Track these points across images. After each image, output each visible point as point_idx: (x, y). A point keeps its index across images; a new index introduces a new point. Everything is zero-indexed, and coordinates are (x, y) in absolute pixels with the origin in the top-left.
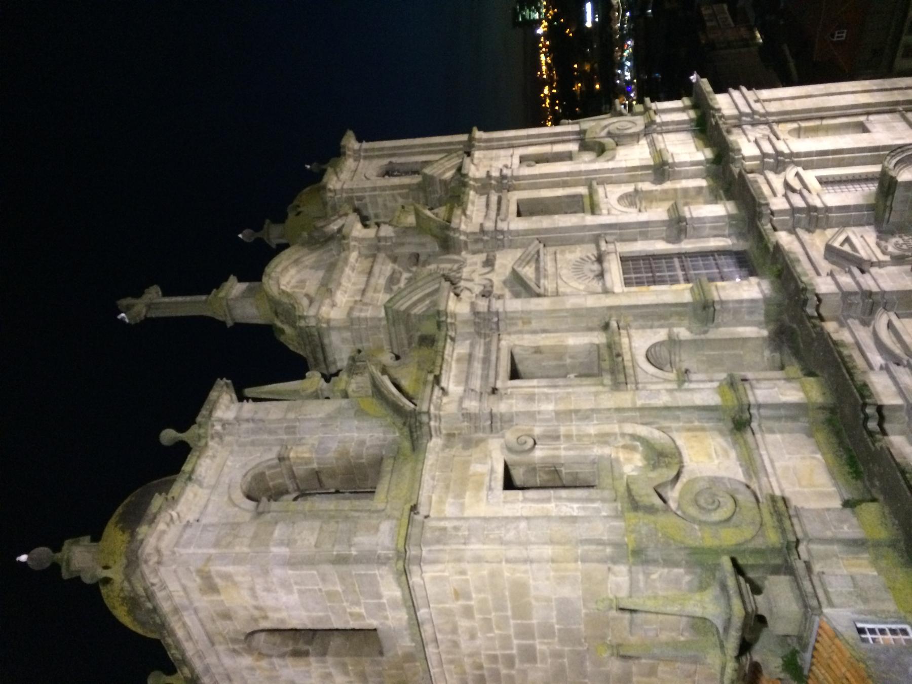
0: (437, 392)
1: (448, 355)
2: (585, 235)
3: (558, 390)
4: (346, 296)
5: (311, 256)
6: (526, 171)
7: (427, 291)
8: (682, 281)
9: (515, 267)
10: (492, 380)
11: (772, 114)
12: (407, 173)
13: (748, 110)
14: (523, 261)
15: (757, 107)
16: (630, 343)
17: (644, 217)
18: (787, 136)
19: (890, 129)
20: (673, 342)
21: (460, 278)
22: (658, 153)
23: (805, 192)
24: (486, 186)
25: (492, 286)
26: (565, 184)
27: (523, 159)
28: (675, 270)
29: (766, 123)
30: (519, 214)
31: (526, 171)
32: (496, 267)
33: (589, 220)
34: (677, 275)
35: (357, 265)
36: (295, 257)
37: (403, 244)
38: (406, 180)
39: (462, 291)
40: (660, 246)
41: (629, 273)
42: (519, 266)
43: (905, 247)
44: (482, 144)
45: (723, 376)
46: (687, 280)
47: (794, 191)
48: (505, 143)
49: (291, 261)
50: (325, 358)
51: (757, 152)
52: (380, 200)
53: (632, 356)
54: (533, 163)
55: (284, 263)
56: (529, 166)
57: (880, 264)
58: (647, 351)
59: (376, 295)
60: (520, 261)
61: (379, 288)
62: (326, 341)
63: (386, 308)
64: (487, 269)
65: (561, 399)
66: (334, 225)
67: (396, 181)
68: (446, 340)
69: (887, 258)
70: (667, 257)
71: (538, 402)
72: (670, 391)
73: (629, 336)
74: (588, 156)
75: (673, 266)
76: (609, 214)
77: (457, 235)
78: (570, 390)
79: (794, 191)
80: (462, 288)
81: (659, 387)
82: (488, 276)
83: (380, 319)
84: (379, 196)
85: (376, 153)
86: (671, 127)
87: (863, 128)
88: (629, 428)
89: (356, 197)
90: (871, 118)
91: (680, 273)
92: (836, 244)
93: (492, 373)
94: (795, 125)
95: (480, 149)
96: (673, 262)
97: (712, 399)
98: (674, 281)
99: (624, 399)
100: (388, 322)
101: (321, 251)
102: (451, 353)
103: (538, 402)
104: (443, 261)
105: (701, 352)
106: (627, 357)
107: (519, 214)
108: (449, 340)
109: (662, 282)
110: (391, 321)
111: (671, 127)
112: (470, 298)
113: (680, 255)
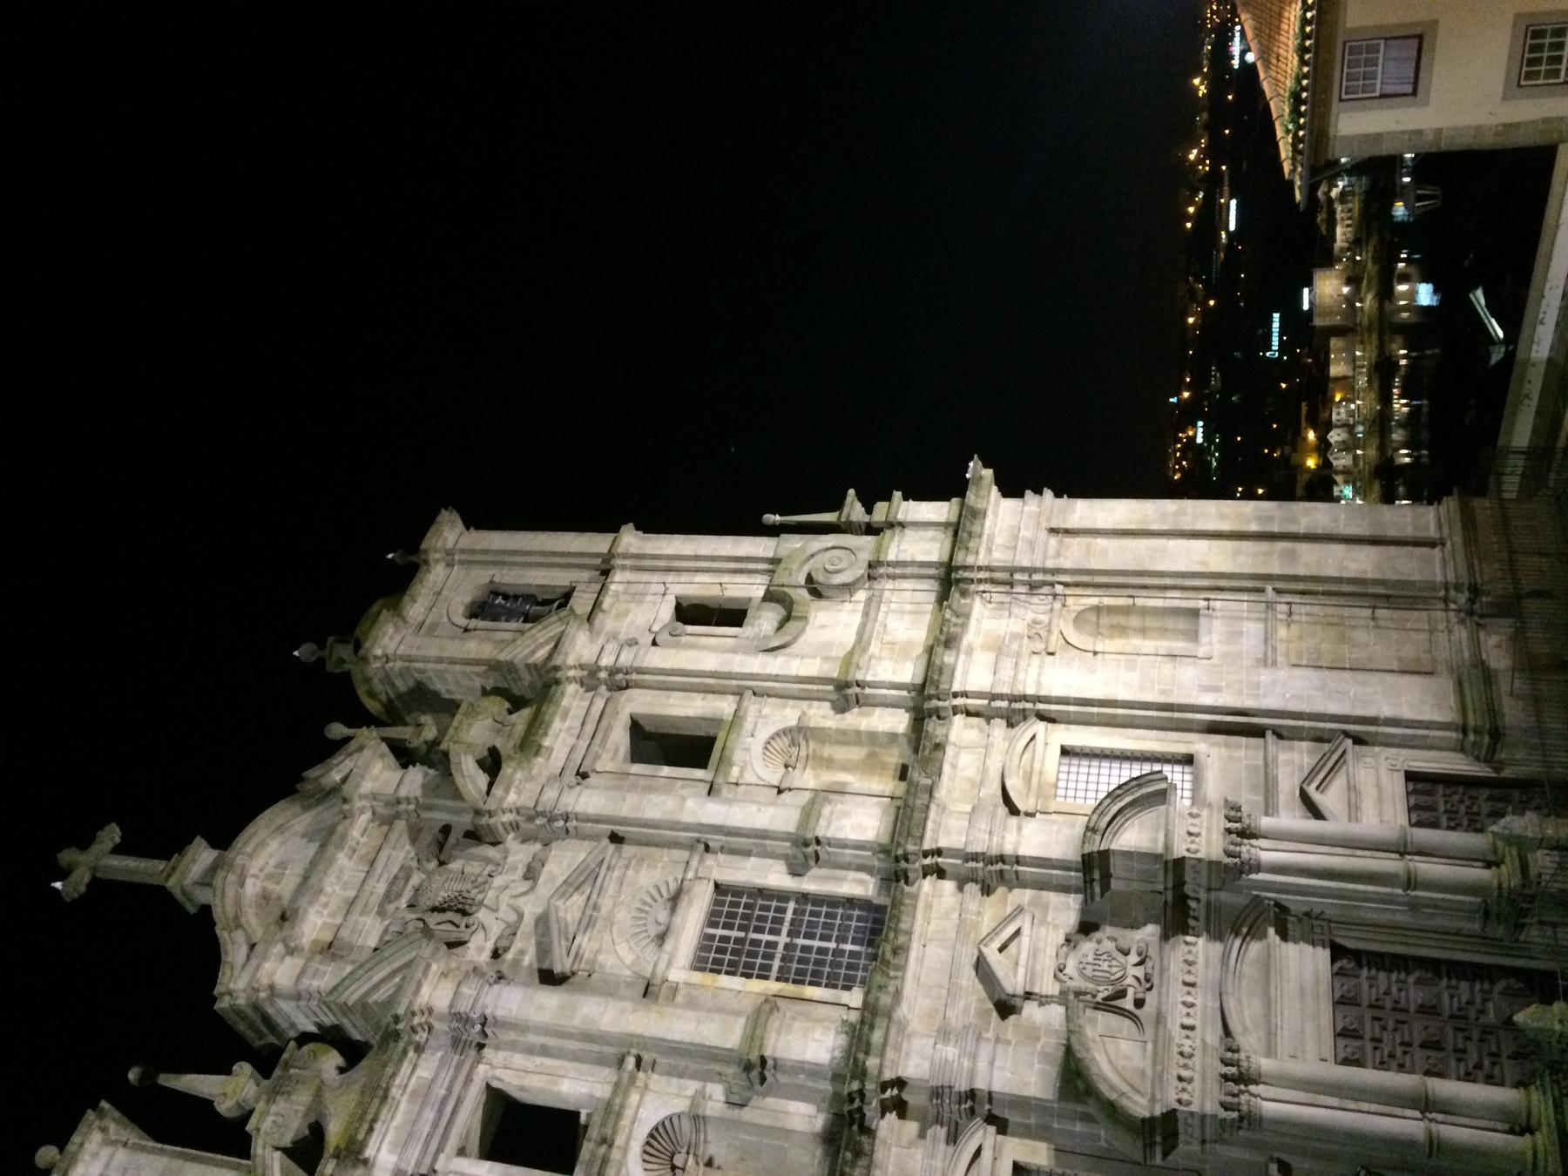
4: (326, 912)
5: (303, 817)
21: (481, 903)
24: (591, 678)
35: (363, 840)
36: (279, 821)
37: (430, 808)
44: (628, 562)
48: (662, 563)
49: (273, 828)
55: (262, 834)
59: (363, 919)
61: (371, 904)
84: (445, 671)
86: (909, 571)
95: (624, 568)
101: (320, 808)
104: (474, 858)
111: (909, 571)
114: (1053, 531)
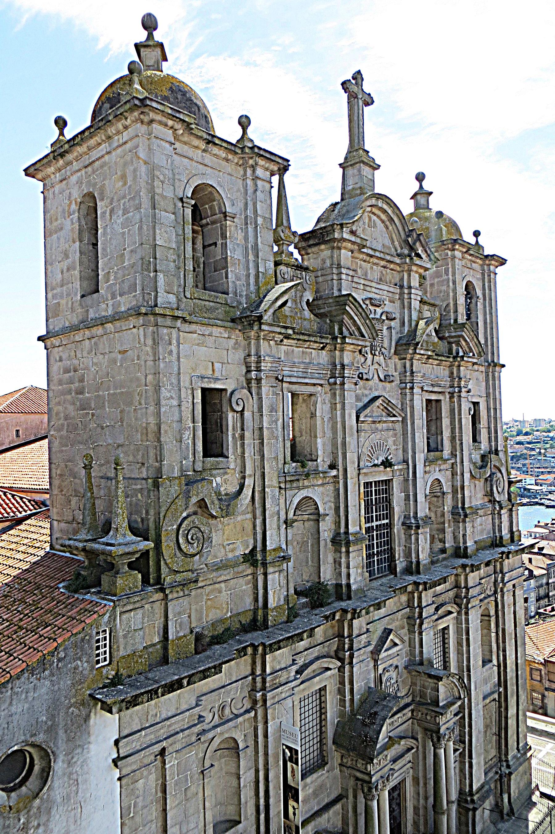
0: (278, 337)
1: (310, 345)
2: (408, 453)
3: (280, 430)
6: (466, 406)
7: (362, 327)
8: (368, 525)
9: (382, 398)
10: (288, 380)
11: (502, 597)
12: (468, 309)
13: (506, 579)
14: (387, 404)
15: (510, 585)
16: (318, 485)
17: (421, 498)
18: (483, 608)
19: (486, 681)
20: (317, 517)
22: (475, 511)
23: (436, 617)
25: (367, 380)
26: (453, 439)
27: (476, 404)
28: (377, 520)
29: (495, 592)
30: (429, 401)
31: (466, 406)
32: (384, 383)
33: (420, 457)
34: (372, 521)
38: (462, 310)
39: (364, 355)
40: (398, 510)
41: (375, 486)
42: (383, 400)
43: (388, 684)
45: (290, 552)
46: (368, 530)
47: (437, 609)
51: (470, 584)
52: (444, 288)
53: (307, 487)
54: (472, 413)
56: (470, 409)
57: (376, 667)
58: (311, 498)
60: (387, 402)
63: (349, 295)
64: (382, 377)
65: (273, 432)
66: (422, 251)
67: (461, 300)
68: (322, 343)
69: (380, 671)
70: (390, 516)
72: (278, 513)
73: (323, 485)
74: (477, 457)
75: (380, 520)
76: (425, 472)
77: (411, 351)
78: (281, 439)
79: (437, 609)
81: (282, 505)
82: (376, 376)
83: (340, 290)
85: (486, 284)
87: (486, 662)
88: (249, 482)
89: (448, 268)
90: (496, 669)
91: (374, 524)
92: (391, 637)
93: (294, 380)
94: (492, 612)
96: (384, 519)
98: (368, 520)
99: (271, 480)
100: (336, 297)
105: (310, 537)
106: (306, 483)
107: (429, 401)
108: (322, 345)
109: (368, 509)
110: (337, 299)
112: (358, 363)
113: (390, 526)
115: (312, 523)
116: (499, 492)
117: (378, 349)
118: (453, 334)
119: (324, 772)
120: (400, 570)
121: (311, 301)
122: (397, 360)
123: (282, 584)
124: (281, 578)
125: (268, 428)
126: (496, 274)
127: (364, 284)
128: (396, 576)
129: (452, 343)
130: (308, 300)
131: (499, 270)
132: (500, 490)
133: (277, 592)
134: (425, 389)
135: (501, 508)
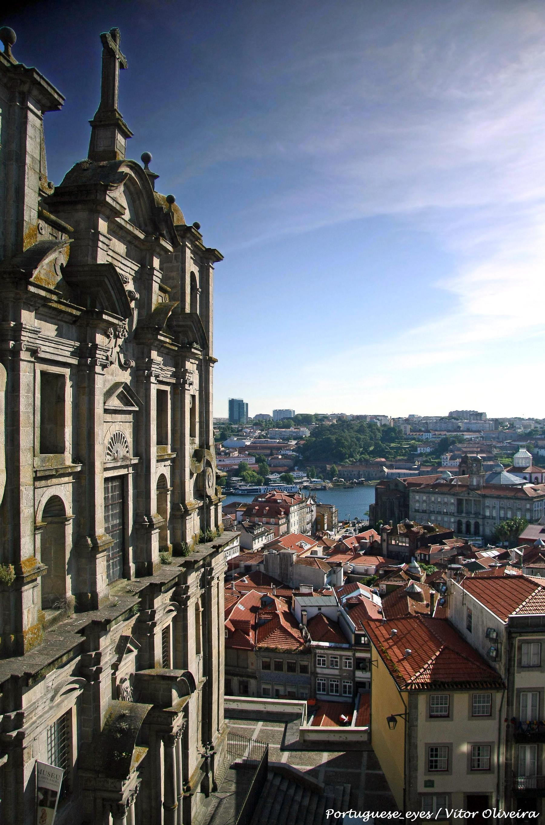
50: (64, 203)
62: (79, 207)
71: (26, 396)
80: (111, 336)
97: (25, 552)
98: (106, 519)
102: (64, 319)
103: (26, 396)
108: (74, 319)
114: (104, 422)
115: (55, 525)
116: (209, 487)
117: (122, 330)
118: (181, 323)
119: (70, 803)
120: (133, 573)
121: (65, 265)
122: (135, 345)
123: (35, 600)
124: (35, 593)
125: (25, 413)
126: (213, 269)
127: (112, 257)
128: (129, 579)
129: (180, 332)
130: (62, 264)
131: (216, 265)
132: (210, 485)
133: (31, 610)
134: (161, 379)
135: (211, 503)
